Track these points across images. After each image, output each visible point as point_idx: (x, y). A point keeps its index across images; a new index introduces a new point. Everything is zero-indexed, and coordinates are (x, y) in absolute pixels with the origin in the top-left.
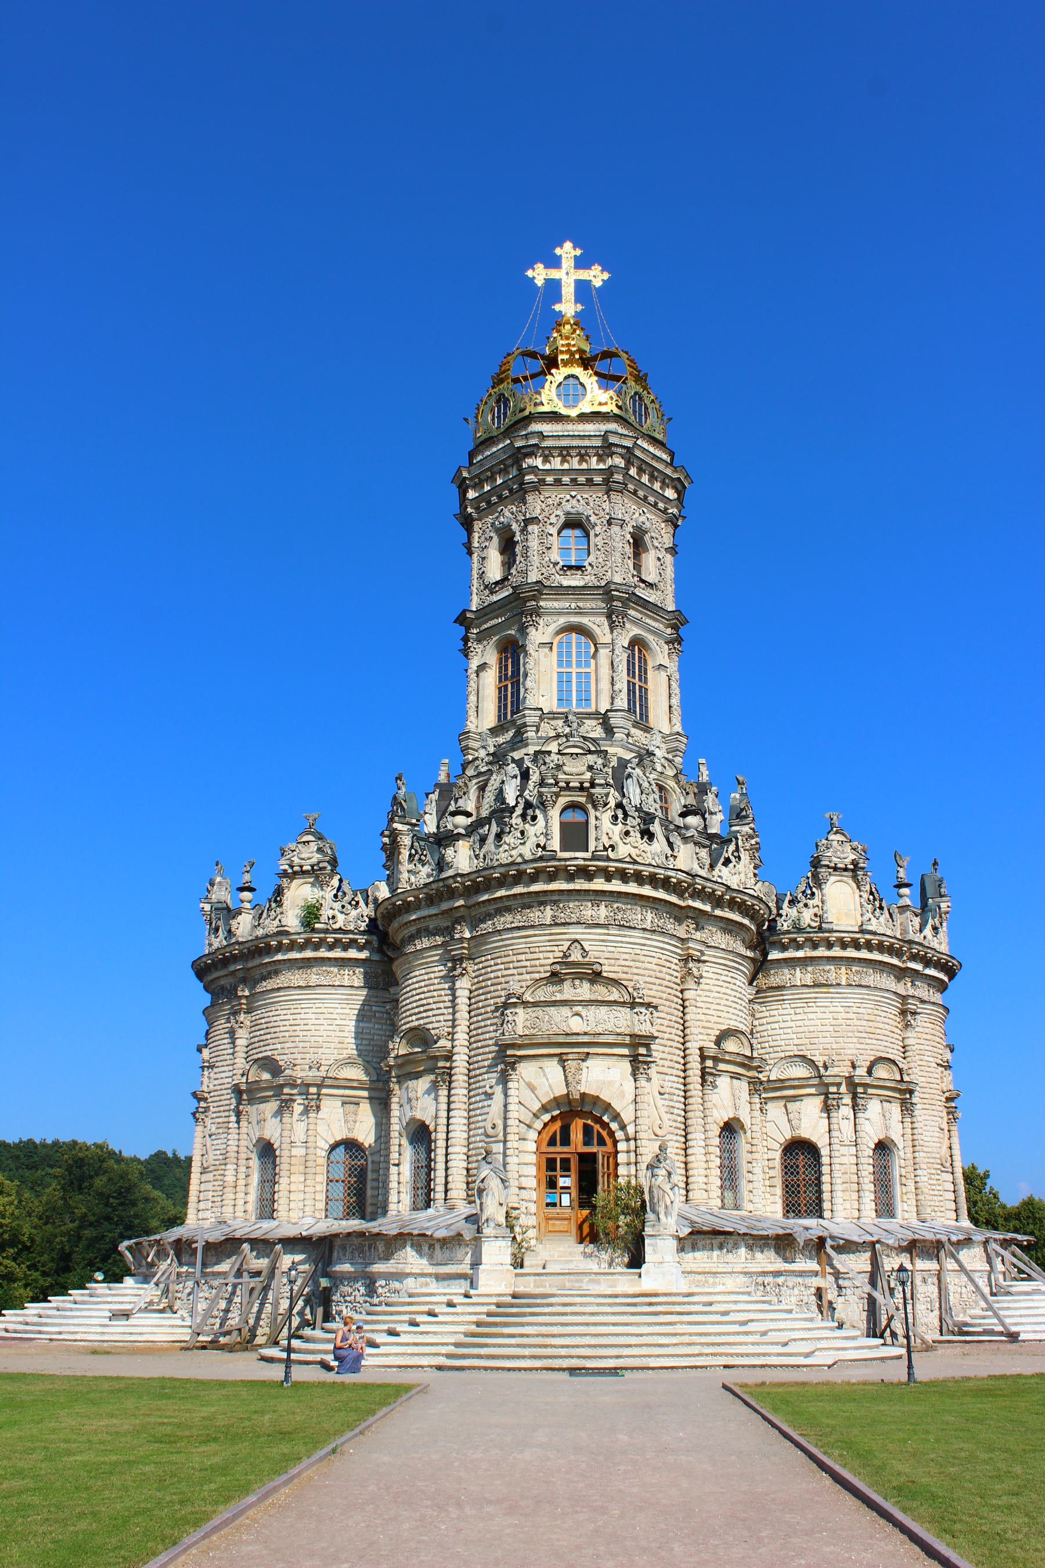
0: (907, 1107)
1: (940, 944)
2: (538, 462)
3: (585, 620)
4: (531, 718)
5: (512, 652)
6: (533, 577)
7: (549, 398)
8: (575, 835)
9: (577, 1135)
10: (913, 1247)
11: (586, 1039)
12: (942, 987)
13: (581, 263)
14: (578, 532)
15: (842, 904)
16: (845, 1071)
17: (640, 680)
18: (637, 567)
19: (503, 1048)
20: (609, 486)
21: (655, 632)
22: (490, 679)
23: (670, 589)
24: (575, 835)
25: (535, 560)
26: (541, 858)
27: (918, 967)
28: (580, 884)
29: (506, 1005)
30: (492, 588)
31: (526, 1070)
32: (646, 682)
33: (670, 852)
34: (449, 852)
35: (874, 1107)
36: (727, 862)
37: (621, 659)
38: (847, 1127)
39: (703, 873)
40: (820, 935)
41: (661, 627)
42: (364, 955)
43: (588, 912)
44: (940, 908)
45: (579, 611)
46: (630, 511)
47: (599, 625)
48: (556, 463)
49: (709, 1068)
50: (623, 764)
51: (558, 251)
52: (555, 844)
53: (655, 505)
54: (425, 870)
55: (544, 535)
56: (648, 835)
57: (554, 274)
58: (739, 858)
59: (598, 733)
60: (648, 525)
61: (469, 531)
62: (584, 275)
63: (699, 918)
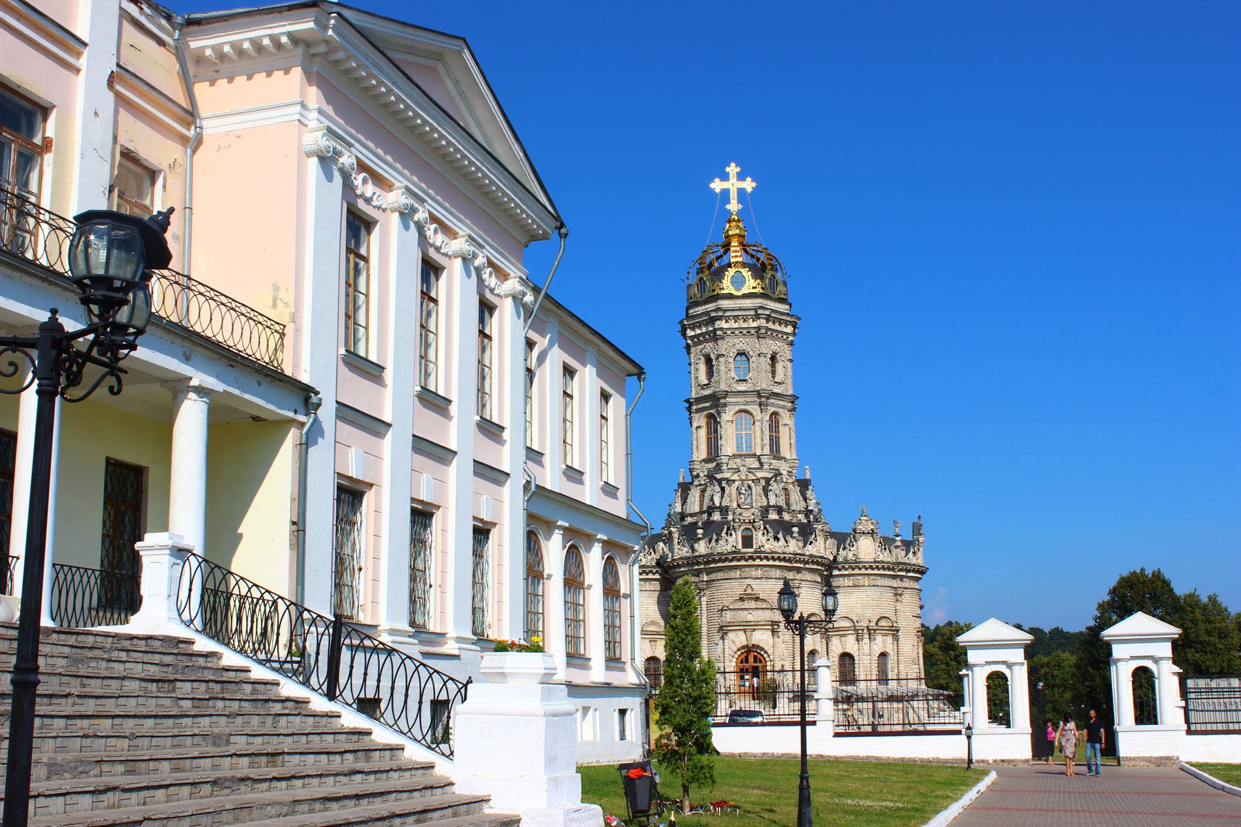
0: (896, 638)
1: (917, 559)
3: (748, 408)
4: (725, 460)
5: (713, 423)
6: (723, 387)
7: (727, 286)
8: (747, 541)
9: (751, 659)
10: (891, 699)
12: (917, 579)
13: (741, 177)
14: (744, 358)
15: (866, 549)
16: (865, 624)
18: (774, 373)
19: (721, 628)
20: (759, 334)
21: (783, 407)
22: (703, 433)
23: (789, 381)
24: (747, 541)
25: (723, 376)
26: (734, 552)
28: (751, 562)
29: (722, 610)
30: (703, 387)
31: (731, 635)
34: (696, 546)
35: (879, 638)
37: (766, 425)
38: (866, 648)
40: (856, 564)
42: (657, 576)
43: (754, 573)
45: (747, 403)
46: (770, 346)
47: (754, 409)
50: (768, 480)
51: (727, 169)
52: (740, 546)
54: (685, 549)
55: (727, 362)
56: (776, 539)
57: (725, 185)
59: (756, 465)
61: (689, 353)
62: (742, 185)
63: (798, 570)
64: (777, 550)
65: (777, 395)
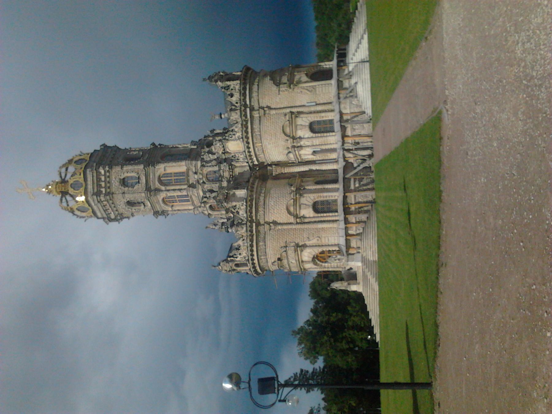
2: (113, 216)
3: (160, 200)
11: (298, 262)
17: (171, 177)
27: (248, 110)
28: (257, 265)
32: (171, 173)
33: (242, 239)
35: (300, 133)
36: (238, 213)
39: (245, 229)
41: (151, 171)
44: (222, 87)
48: (110, 211)
49: (301, 220)
53: (109, 177)
58: (235, 206)
60: (117, 179)
64: (245, 247)
65: (147, 181)
